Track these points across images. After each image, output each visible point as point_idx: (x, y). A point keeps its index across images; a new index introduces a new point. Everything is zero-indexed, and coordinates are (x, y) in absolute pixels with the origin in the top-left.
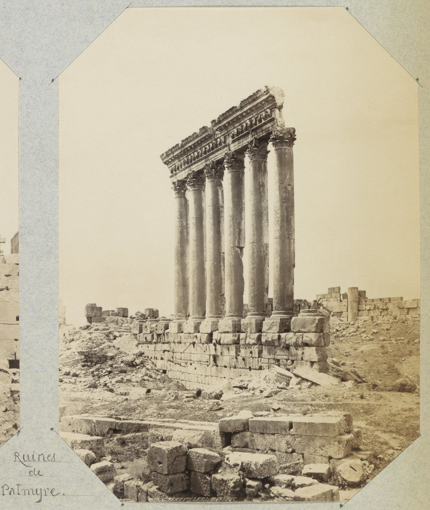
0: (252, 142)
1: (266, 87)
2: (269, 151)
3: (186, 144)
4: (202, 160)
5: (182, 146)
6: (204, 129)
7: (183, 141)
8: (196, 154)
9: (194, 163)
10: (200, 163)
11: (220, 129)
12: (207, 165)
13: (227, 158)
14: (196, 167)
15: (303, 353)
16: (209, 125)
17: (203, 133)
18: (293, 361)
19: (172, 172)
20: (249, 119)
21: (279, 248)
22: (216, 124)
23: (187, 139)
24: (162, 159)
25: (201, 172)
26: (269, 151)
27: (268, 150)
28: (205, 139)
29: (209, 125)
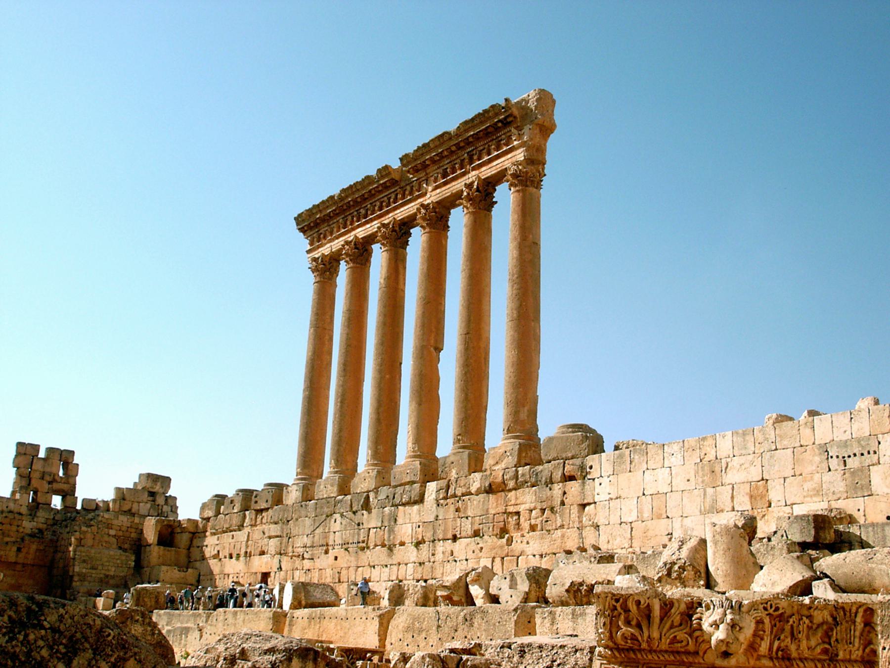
0: (473, 182)
1: (506, 100)
2: (496, 202)
3: (347, 197)
4: (372, 220)
5: (341, 198)
6: (385, 171)
7: (343, 191)
8: (363, 211)
9: (359, 226)
10: (368, 226)
11: (416, 170)
12: (384, 225)
13: (423, 211)
14: (361, 233)
15: (565, 493)
16: (396, 164)
17: (383, 177)
18: (543, 511)
19: (311, 244)
20: (468, 153)
21: (516, 336)
22: (409, 163)
23: (351, 187)
24: (298, 224)
25: (370, 240)
26: (496, 202)
27: (494, 200)
28: (385, 187)
29: (396, 164)
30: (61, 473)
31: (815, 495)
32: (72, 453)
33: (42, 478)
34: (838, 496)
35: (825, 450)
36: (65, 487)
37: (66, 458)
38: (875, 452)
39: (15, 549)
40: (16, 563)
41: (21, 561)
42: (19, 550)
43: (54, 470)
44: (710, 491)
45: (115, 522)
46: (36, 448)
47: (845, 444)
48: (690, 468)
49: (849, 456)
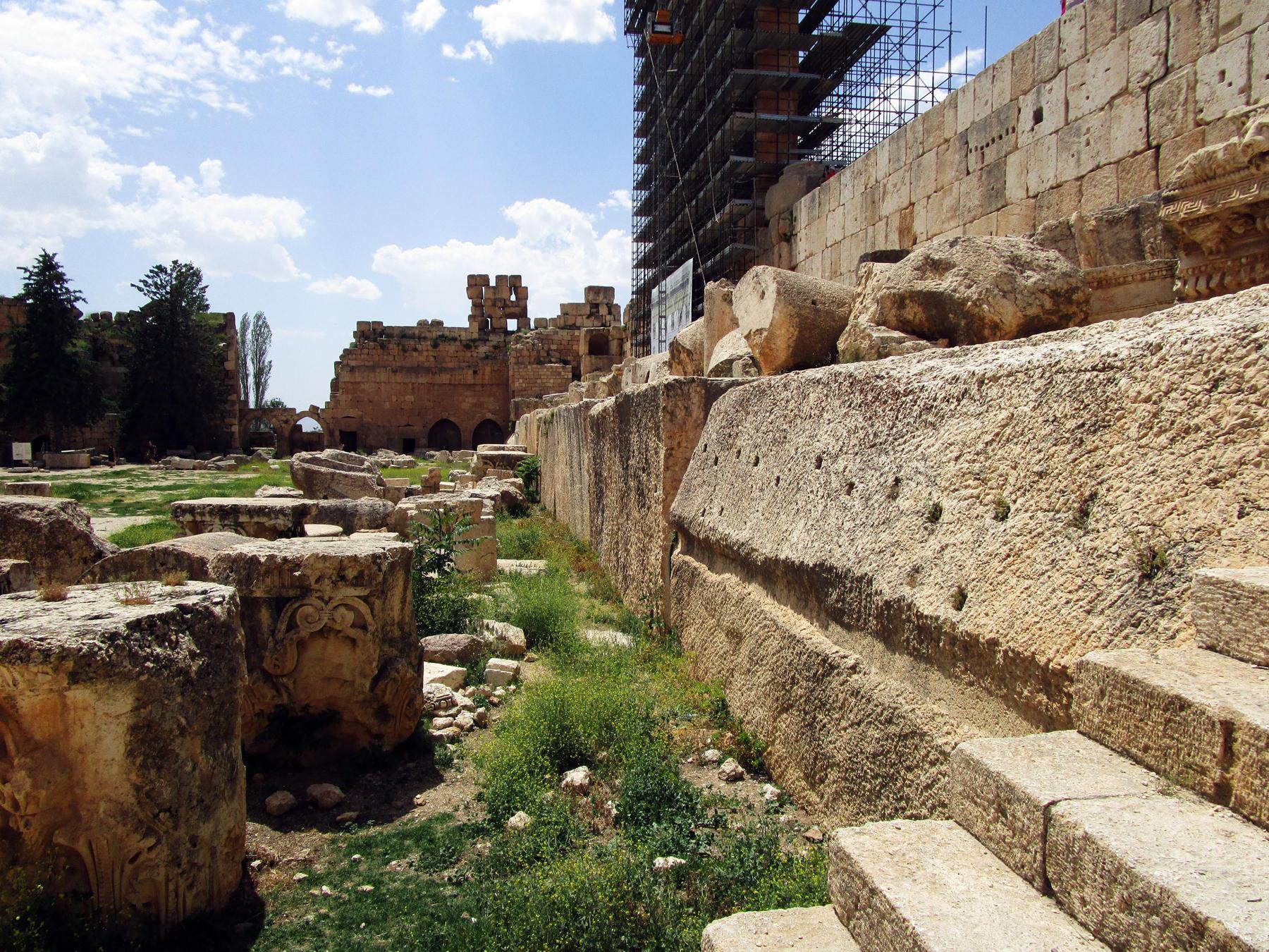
30: (513, 298)
31: (952, 217)
32: (518, 278)
33: (494, 305)
34: (973, 214)
35: (964, 138)
36: (517, 310)
37: (514, 283)
38: (1014, 129)
39: (471, 372)
41: (479, 382)
42: (475, 372)
43: (505, 296)
44: (870, 229)
45: (555, 337)
46: (485, 279)
47: (983, 126)
48: (858, 198)
49: (988, 145)
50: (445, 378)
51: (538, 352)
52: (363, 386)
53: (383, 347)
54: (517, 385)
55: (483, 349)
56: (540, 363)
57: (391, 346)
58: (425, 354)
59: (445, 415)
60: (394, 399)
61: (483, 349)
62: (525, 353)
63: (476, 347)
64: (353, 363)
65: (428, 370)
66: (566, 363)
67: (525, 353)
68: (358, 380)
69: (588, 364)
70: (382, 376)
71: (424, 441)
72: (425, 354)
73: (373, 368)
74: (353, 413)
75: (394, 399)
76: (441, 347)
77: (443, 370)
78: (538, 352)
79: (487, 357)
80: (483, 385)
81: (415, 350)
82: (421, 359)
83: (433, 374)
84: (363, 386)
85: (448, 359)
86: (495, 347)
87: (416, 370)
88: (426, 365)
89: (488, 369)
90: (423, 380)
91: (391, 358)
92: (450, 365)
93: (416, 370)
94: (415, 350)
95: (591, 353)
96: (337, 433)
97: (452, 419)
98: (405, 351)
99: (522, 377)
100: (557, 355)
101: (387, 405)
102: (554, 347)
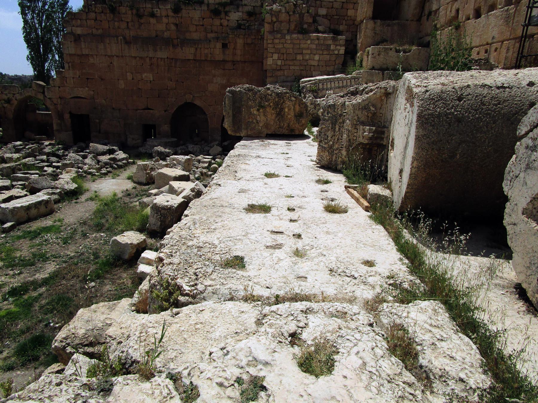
39: (219, 45)
40: (224, 61)
42: (225, 46)
50: (188, 52)
51: (301, 16)
52: (91, 60)
53: (113, 10)
54: (270, 61)
55: (235, 16)
56: (303, 32)
57: (123, 9)
58: (165, 20)
59: (189, 98)
60: (129, 77)
61: (235, 16)
62: (283, 17)
63: (226, 13)
64: (79, 31)
65: (168, 42)
66: (337, 33)
67: (283, 17)
68: (86, 52)
69: (369, 33)
70: (114, 48)
71: (166, 128)
72: (165, 20)
73: (101, 38)
74: (83, 92)
75: (129, 77)
76: (184, 13)
77: (185, 42)
78: (301, 16)
79: (239, 26)
80: (234, 62)
81: (153, 15)
82: (161, 27)
83: (175, 46)
84: (91, 60)
85: (192, 28)
86: (250, 14)
87: (155, 41)
88: (166, 34)
89: (240, 42)
90: (162, 54)
91: (123, 25)
92: (195, 36)
93: (155, 41)
94: (153, 15)
95: (375, 17)
96: (67, 116)
97: (198, 103)
98: (139, 16)
99: (278, 51)
100: (326, 22)
101: (122, 85)
102: (323, 11)
